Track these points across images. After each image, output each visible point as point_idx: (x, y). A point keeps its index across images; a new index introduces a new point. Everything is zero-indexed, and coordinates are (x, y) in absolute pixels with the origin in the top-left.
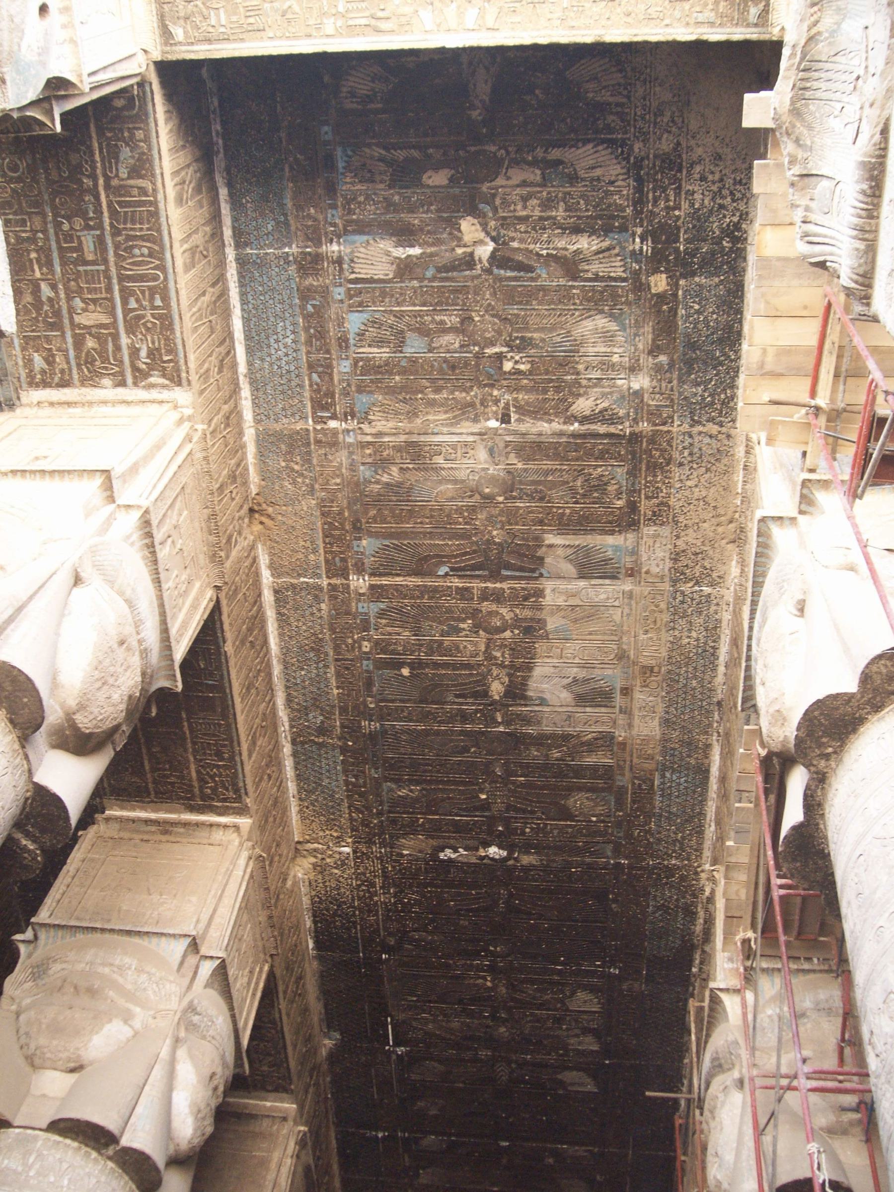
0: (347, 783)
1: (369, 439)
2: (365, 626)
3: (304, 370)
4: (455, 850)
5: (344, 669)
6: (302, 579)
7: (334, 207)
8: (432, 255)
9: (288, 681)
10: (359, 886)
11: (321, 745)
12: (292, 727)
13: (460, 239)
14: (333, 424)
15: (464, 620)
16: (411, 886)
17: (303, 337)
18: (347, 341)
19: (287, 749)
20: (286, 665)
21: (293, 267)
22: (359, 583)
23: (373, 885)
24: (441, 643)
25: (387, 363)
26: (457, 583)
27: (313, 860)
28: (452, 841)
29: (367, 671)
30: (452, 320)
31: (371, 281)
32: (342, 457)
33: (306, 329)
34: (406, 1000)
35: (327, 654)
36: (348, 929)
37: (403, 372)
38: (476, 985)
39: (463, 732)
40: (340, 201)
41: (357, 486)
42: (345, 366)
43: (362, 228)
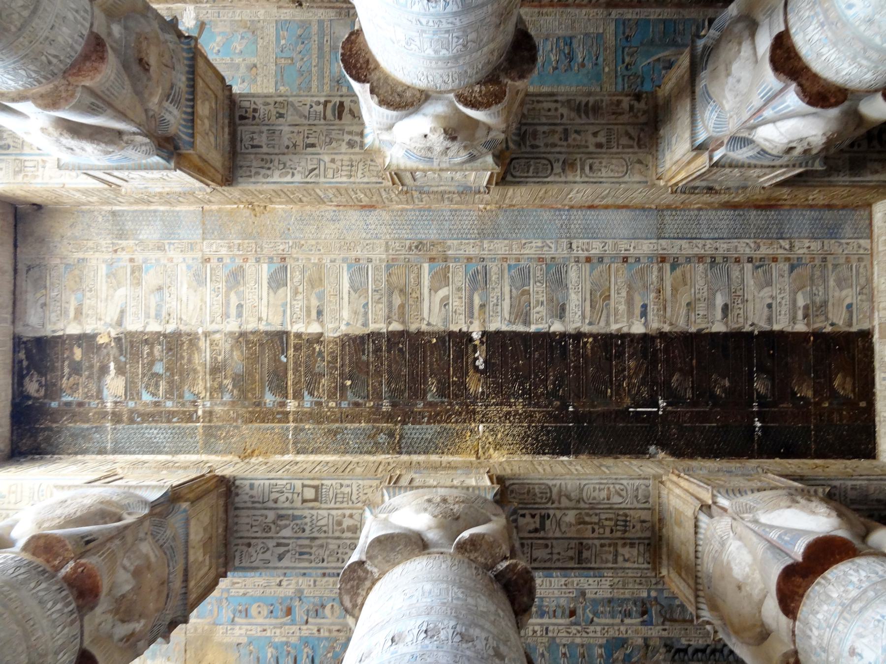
0: (428, 423)
1: (208, 394)
2: (319, 404)
3: (171, 425)
4: (477, 359)
5: (344, 417)
6: (290, 437)
7: (89, 403)
8: (115, 358)
9: (356, 452)
10: (510, 422)
11: (401, 437)
12: (388, 453)
13: (107, 344)
14: (200, 413)
15: (314, 349)
16: (509, 388)
17: (153, 425)
18: (156, 402)
19: (404, 458)
20: (346, 452)
21: (118, 426)
22: (292, 405)
23: (509, 413)
24: (329, 362)
25: (168, 383)
26: (291, 352)
27: (491, 450)
28: (470, 360)
29: (349, 404)
30: (146, 350)
31: (126, 387)
32: (218, 409)
33: (150, 422)
34: (611, 397)
35: (338, 428)
36: (549, 432)
37: (172, 375)
38: (592, 349)
39: (389, 351)
40: (87, 400)
41: (233, 403)
42: (169, 404)
43: (100, 391)
